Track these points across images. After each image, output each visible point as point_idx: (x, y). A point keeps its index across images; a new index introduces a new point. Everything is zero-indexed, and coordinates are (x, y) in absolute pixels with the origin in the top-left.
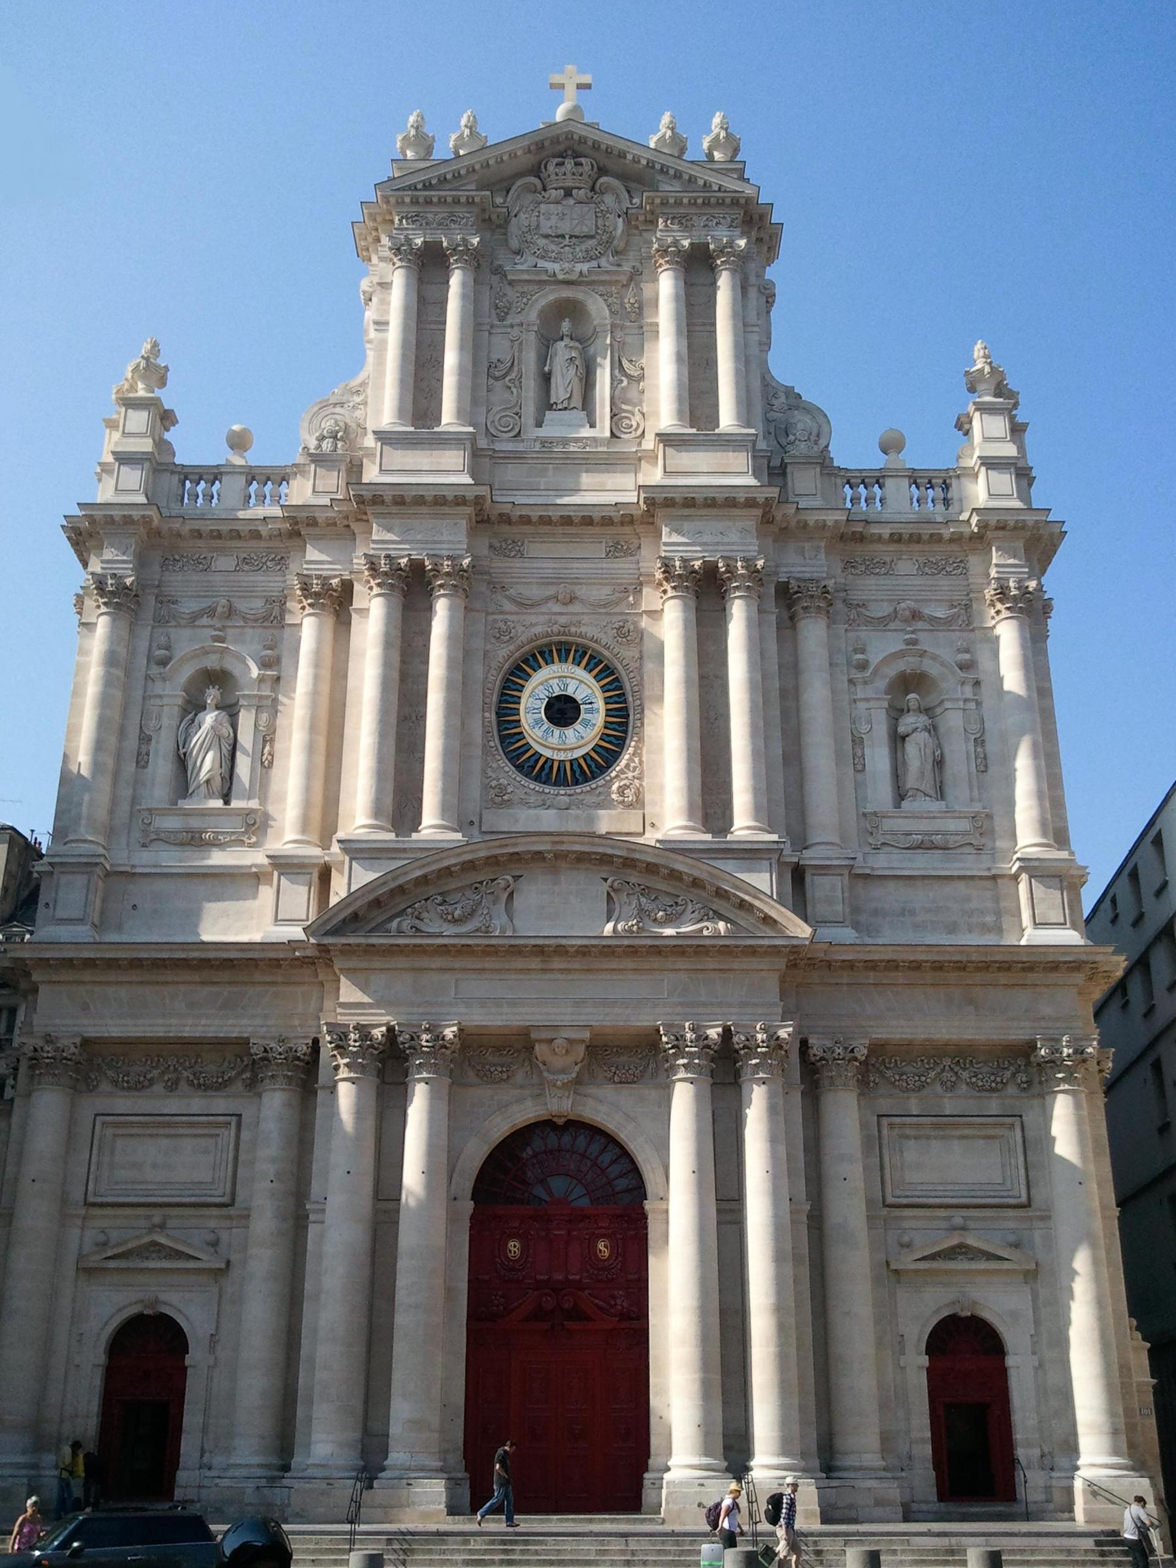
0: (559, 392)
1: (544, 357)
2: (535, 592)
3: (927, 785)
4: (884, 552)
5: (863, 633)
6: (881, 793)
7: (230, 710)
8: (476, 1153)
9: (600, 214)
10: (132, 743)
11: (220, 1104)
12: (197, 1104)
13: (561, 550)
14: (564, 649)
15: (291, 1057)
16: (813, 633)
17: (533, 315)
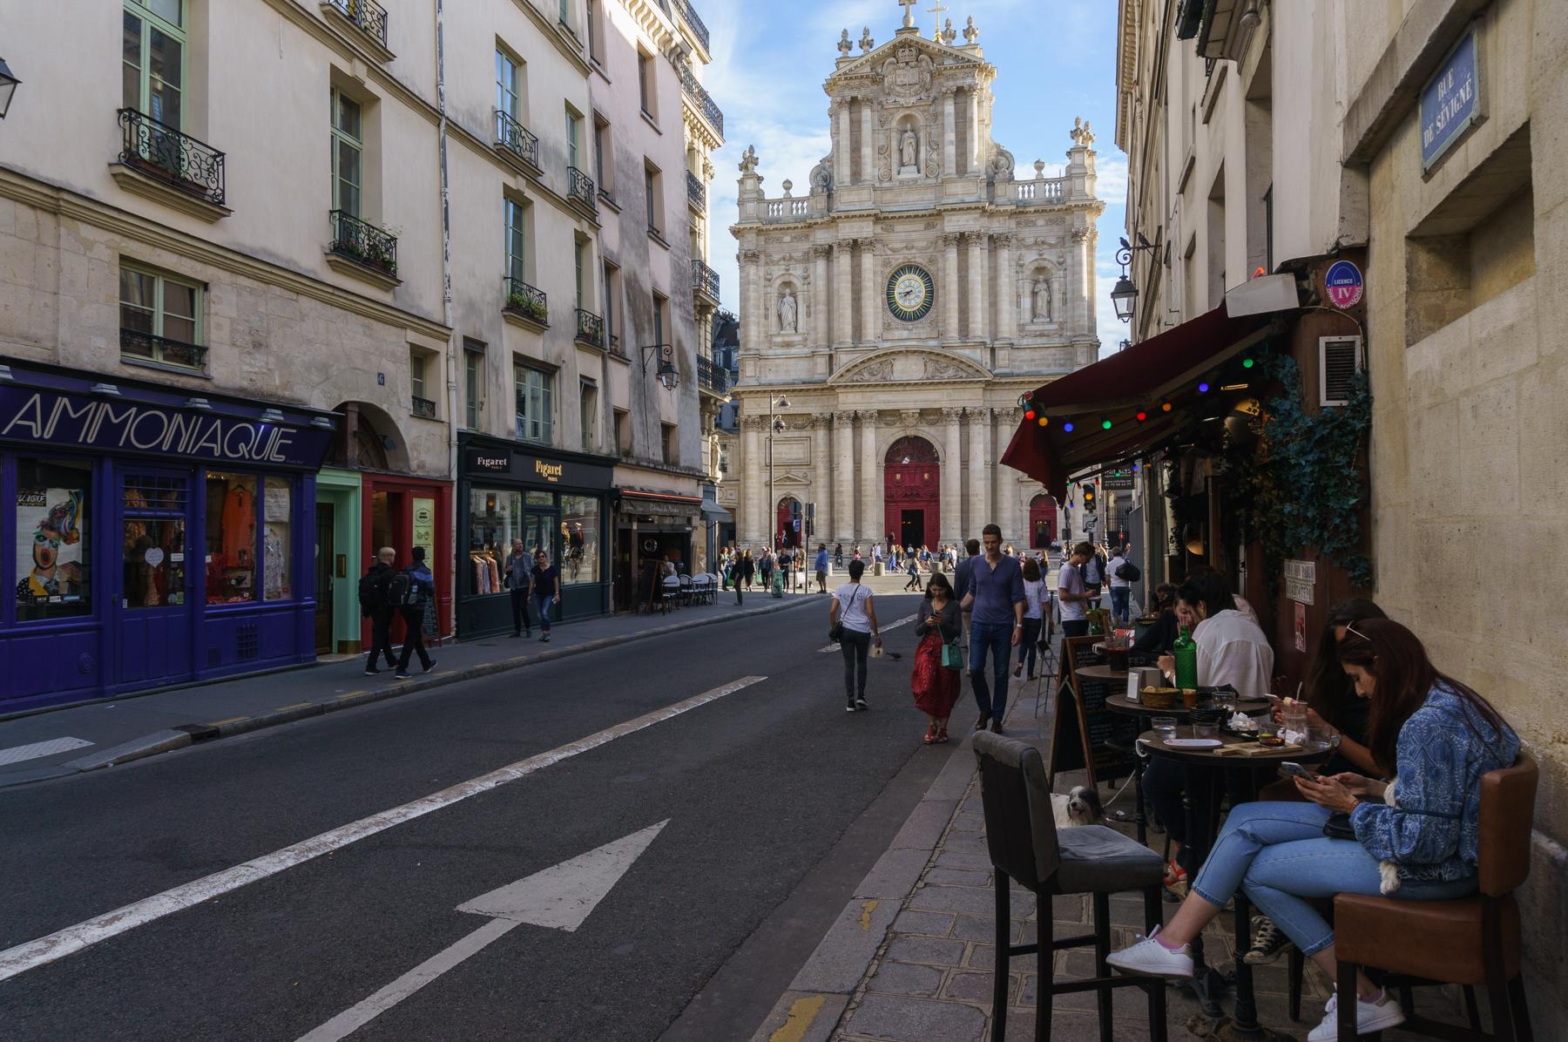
0: (906, 159)
1: (900, 141)
2: (898, 246)
3: (1045, 312)
4: (1033, 217)
5: (1023, 252)
6: (1027, 316)
7: (794, 295)
8: (885, 449)
9: (921, 73)
10: (762, 311)
11: (804, 434)
12: (797, 434)
13: (908, 227)
14: (910, 268)
15: (824, 419)
16: (1004, 255)
17: (894, 124)
